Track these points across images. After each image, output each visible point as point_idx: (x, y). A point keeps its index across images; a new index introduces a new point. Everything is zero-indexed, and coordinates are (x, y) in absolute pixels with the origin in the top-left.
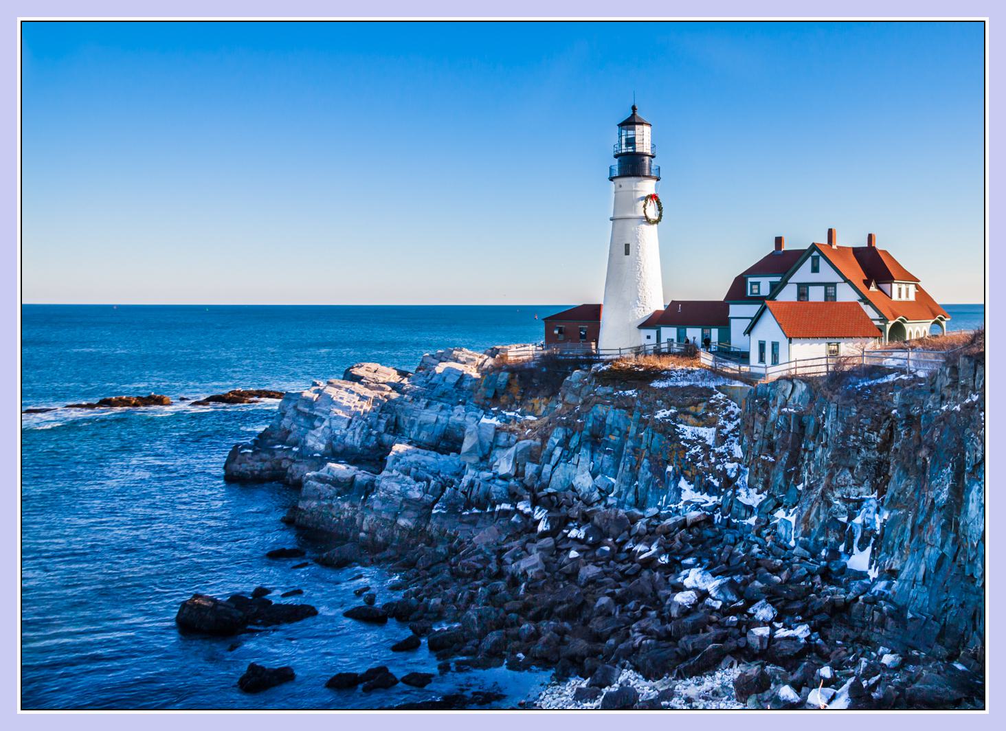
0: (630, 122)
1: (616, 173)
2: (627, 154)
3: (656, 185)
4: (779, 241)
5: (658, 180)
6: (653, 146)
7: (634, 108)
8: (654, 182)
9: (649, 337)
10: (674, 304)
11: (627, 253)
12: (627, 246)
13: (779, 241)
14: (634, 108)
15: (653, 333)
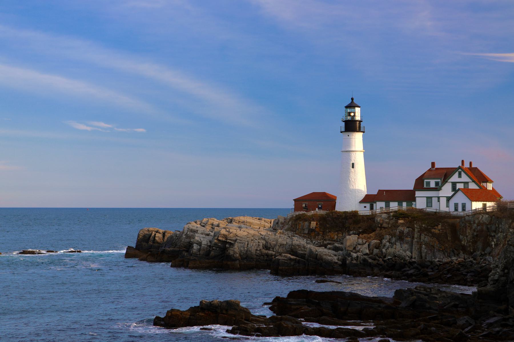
0: (352, 106)
1: (343, 130)
2: (349, 121)
3: (363, 135)
4: (433, 164)
5: (364, 132)
6: (361, 116)
7: (352, 99)
8: (362, 133)
9: (365, 207)
10: (380, 192)
11: (353, 167)
12: (353, 164)
13: (433, 164)
14: (352, 99)
15: (368, 205)
